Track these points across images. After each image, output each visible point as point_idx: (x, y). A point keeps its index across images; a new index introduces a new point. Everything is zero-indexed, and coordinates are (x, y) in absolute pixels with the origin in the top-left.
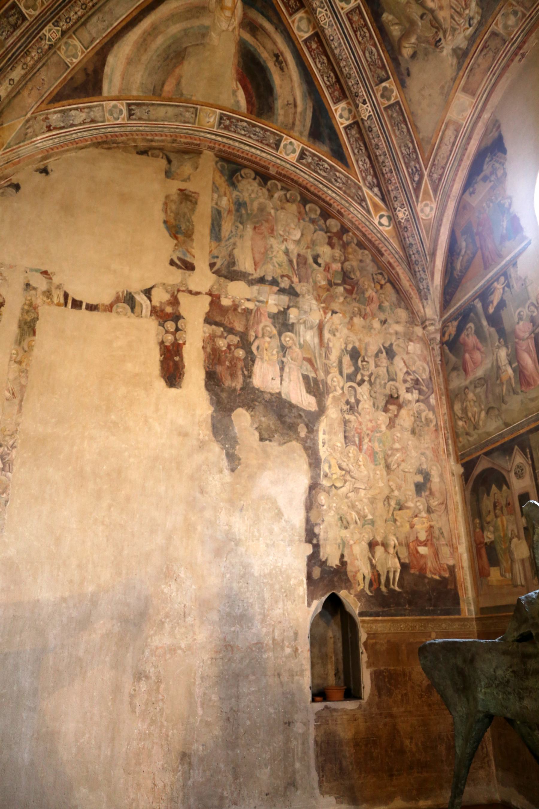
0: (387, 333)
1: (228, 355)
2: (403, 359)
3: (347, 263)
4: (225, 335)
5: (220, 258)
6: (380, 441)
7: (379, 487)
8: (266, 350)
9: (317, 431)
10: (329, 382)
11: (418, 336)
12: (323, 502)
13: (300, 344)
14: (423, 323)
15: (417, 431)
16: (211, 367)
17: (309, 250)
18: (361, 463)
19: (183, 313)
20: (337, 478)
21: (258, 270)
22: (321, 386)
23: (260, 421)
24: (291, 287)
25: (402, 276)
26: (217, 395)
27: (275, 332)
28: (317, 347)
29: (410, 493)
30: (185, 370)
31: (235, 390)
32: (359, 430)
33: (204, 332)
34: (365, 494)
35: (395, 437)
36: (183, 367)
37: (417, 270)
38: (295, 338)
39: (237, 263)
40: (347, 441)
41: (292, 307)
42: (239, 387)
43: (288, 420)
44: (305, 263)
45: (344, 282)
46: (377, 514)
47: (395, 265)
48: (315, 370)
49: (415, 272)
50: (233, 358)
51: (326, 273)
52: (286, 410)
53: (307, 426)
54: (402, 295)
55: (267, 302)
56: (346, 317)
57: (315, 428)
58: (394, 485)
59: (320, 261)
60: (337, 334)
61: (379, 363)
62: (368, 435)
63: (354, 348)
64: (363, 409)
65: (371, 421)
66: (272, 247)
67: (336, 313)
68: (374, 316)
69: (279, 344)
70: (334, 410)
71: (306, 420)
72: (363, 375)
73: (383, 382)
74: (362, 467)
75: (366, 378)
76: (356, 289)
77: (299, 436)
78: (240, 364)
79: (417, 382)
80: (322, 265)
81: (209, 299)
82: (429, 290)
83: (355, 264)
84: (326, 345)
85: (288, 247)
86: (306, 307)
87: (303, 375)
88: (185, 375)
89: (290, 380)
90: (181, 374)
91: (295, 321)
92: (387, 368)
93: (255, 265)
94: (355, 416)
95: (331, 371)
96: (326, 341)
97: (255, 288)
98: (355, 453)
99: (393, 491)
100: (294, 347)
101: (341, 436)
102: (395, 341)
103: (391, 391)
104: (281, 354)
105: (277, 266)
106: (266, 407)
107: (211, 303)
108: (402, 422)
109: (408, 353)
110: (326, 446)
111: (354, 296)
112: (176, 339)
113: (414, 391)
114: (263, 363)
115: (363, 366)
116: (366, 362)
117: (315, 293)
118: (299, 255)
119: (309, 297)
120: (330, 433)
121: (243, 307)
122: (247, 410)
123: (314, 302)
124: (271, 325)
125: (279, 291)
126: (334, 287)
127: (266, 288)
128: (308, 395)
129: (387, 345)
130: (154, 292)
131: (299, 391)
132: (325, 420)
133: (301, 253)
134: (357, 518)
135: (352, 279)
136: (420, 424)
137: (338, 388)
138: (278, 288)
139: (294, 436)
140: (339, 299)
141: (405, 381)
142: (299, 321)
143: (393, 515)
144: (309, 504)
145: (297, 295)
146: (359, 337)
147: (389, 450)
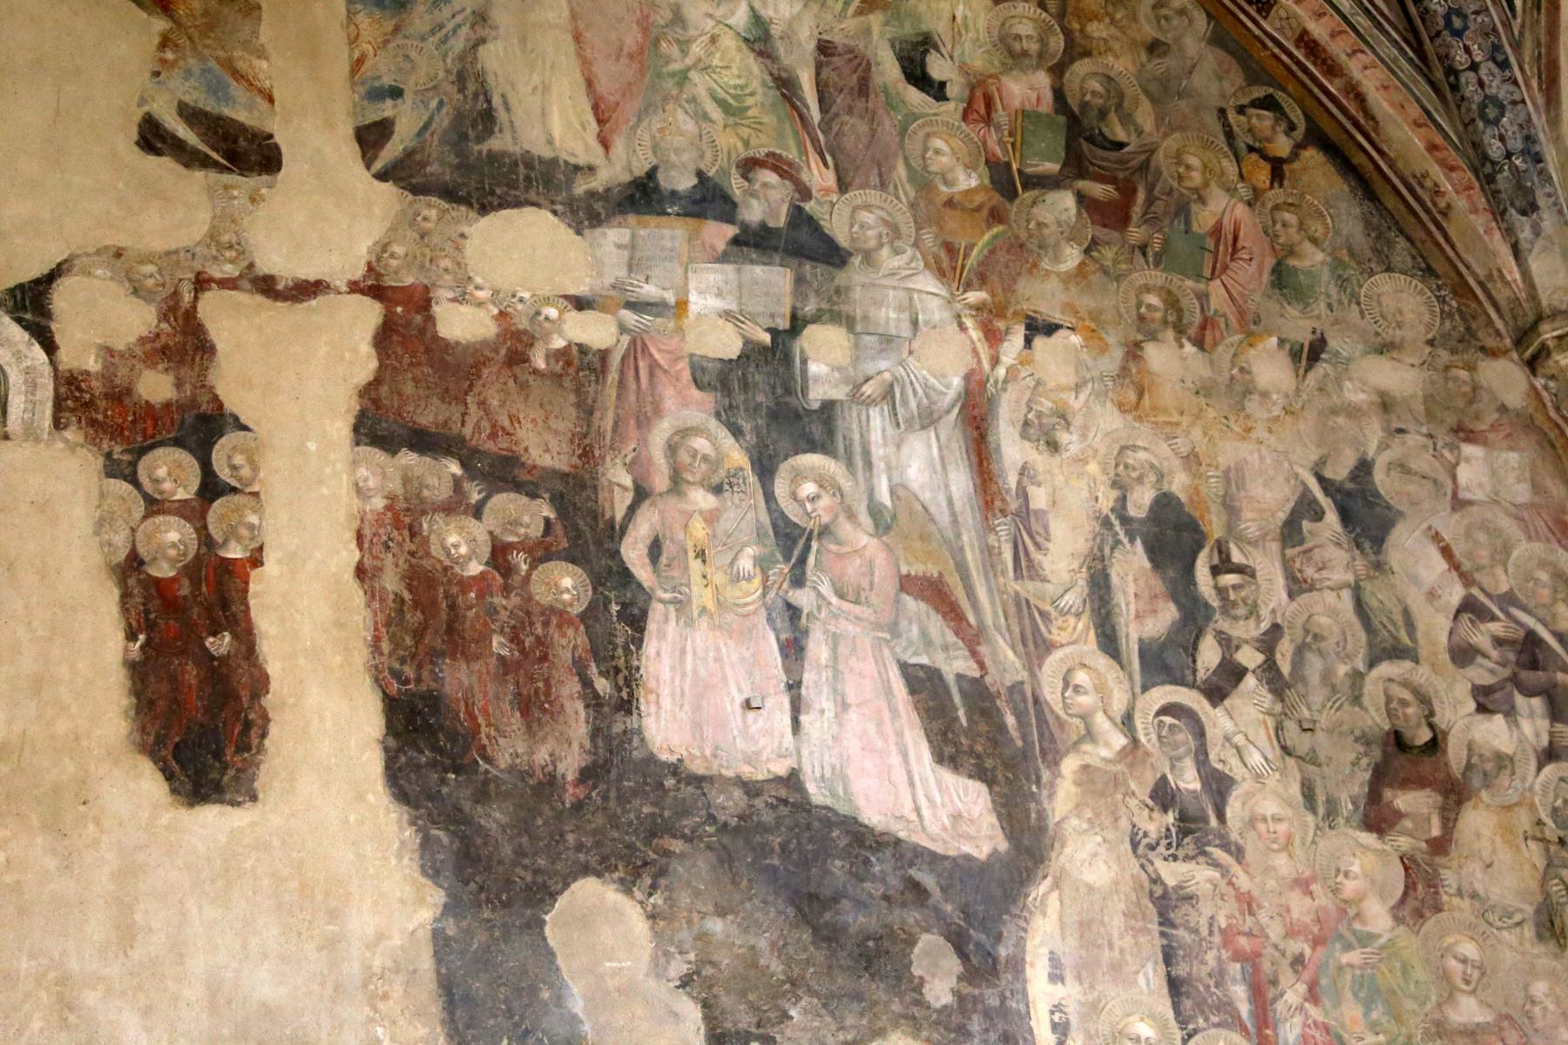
0: (1335, 411)
1: (498, 600)
2: (1436, 537)
3: (1080, 68)
4: (475, 497)
5: (409, 96)
6: (1369, 992)
8: (701, 555)
9: (1017, 965)
10: (1051, 692)
11: (1503, 408)
13: (875, 511)
14: (1523, 336)
16: (409, 671)
17: (875, 20)
19: (234, 400)
21: (619, 146)
22: (1010, 720)
23: (703, 937)
24: (799, 218)
25: (1380, 102)
26: (454, 818)
27: (737, 456)
28: (970, 519)
30: (268, 701)
31: (551, 782)
32: (1243, 941)
33: (360, 491)
35: (1453, 964)
36: (261, 683)
37: (1460, 58)
38: (846, 484)
39: (501, 115)
40: (1187, 1004)
41: (816, 319)
42: (570, 765)
43: (855, 920)
44: (863, 88)
45: (1076, 166)
47: (1338, 49)
48: (973, 639)
49: (1451, 71)
50: (527, 613)
51: (974, 131)
52: (837, 866)
53: (959, 942)
54: (1390, 202)
55: (682, 305)
56: (1104, 349)
57: (1003, 952)
59: (938, 68)
60: (1063, 437)
61: (1310, 572)
62: (1298, 961)
63: (1165, 502)
64: (1252, 822)
65: (1303, 885)
66: (678, 18)
67: (1050, 329)
68: (1251, 326)
69: (765, 518)
70: (1093, 842)
71: (949, 908)
72: (1225, 641)
73: (1342, 670)
75: (1249, 657)
76: (1141, 195)
77: (920, 1003)
78: (569, 643)
79: (1529, 651)
80: (951, 91)
81: (370, 314)
82: (1538, 159)
83: (1122, 65)
84: (1013, 505)
85: (767, 13)
86: (890, 316)
87: (905, 668)
88: (274, 730)
89: (844, 706)
90: (248, 725)
91: (839, 393)
92: (1357, 590)
93: (600, 121)
94: (1215, 864)
95: (1057, 636)
96: (1012, 481)
97: (613, 236)
100: (845, 528)
101: (1150, 979)
102: (1384, 446)
103: (1390, 714)
104: (782, 568)
105: (716, 113)
106: (726, 859)
107: (384, 338)
108: (1477, 878)
109: (1458, 504)
111: (1136, 233)
112: (206, 540)
113: (1520, 700)
114: (690, 623)
115: (1221, 591)
116: (1240, 570)
117: (928, 237)
118: (825, 49)
119: (897, 262)
120: (1086, 971)
121: (558, 343)
122: (627, 887)
123: (928, 283)
124: (713, 423)
125: (736, 241)
126: (1027, 196)
127: (668, 233)
128: (948, 777)
129: (1340, 471)
130: (62, 298)
131: (896, 760)
132: (1053, 901)
133: (838, 39)
135: (1120, 145)
137: (1101, 722)
138: (731, 231)
139: (896, 1007)
140: (1057, 259)
141: (1463, 655)
142: (857, 387)
145: (833, 255)
146: (1182, 445)
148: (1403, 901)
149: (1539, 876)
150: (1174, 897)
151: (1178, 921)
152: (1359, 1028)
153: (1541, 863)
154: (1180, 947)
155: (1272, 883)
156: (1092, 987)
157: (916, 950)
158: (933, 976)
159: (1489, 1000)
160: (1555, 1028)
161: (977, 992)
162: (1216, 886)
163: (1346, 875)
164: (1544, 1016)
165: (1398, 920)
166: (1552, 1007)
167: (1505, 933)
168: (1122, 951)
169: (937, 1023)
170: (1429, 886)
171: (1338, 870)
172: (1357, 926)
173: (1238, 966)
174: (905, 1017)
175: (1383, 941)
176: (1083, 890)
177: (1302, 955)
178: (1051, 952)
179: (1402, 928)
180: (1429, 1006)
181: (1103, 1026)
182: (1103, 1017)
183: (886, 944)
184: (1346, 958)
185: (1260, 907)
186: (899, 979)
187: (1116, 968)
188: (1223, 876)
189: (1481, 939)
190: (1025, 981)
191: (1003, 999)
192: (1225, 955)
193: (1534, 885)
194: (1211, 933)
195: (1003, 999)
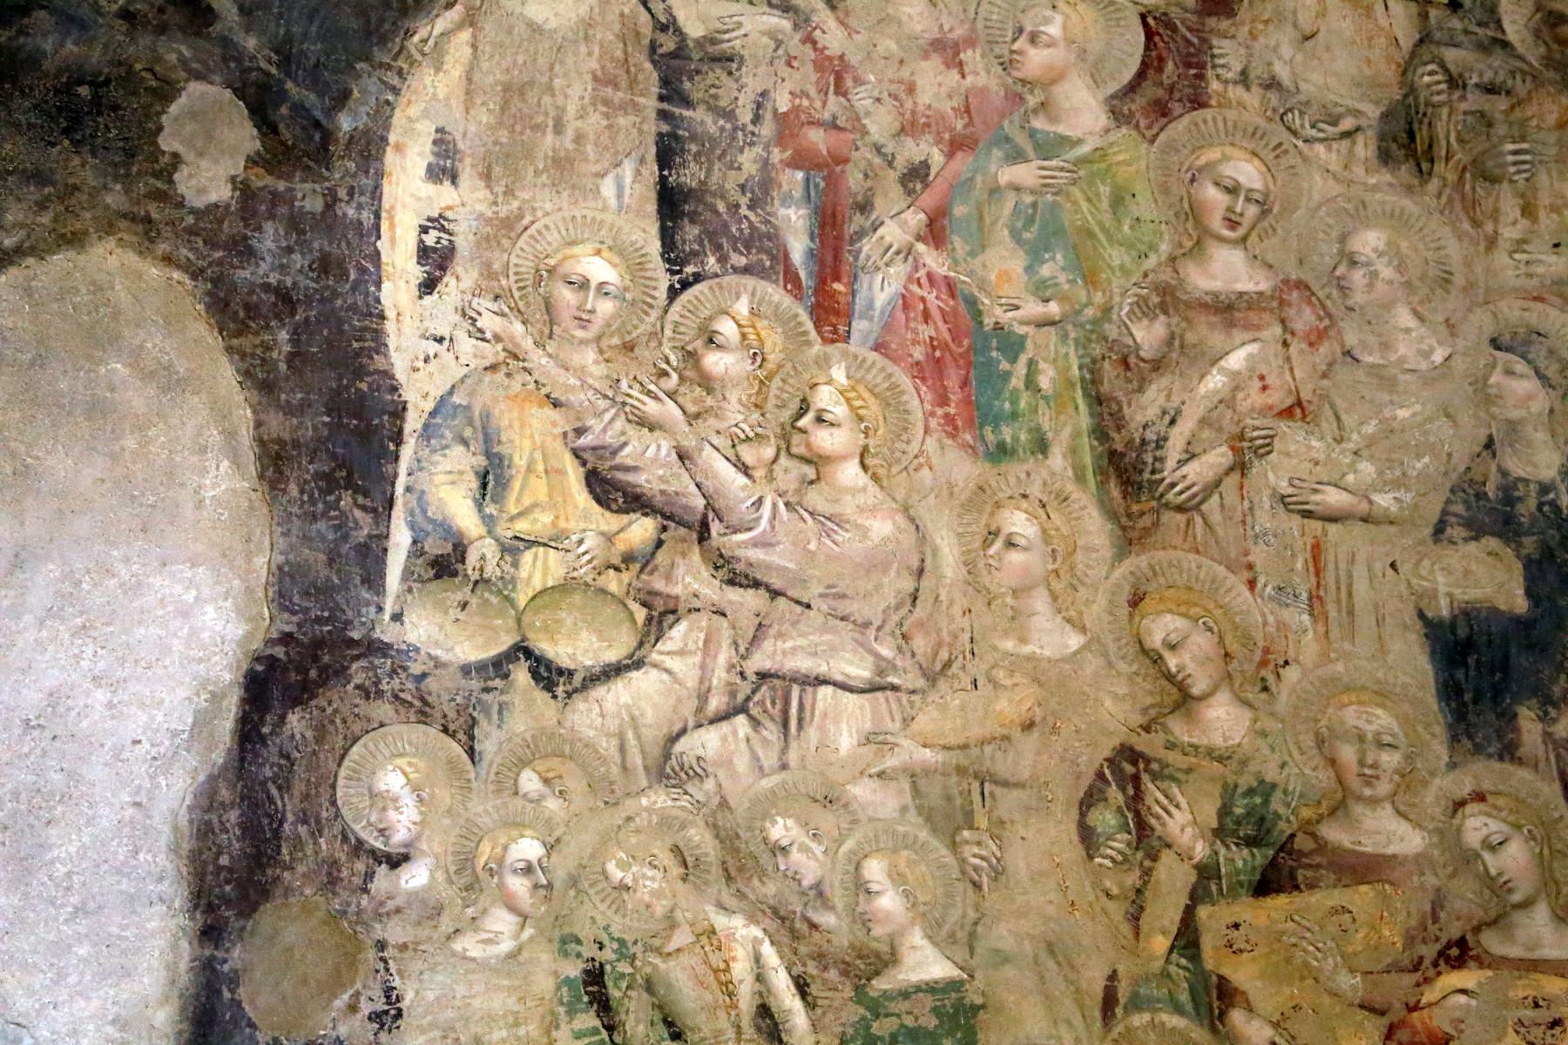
7: (1035, 670)
12: (403, 822)
15: (1445, 128)
18: (826, 440)
20: (566, 587)
29: (1382, 720)
34: (874, 739)
35: (1212, 195)
40: (690, 232)
46: (1002, 936)
57: (345, 123)
58: (1201, 642)
62: (916, 175)
71: (251, 43)
74: (850, 473)
98: (774, 342)
99: (1183, 700)
108: (1284, 60)
110: (453, 288)
134: (781, 982)
136: (1491, 68)
139: (115, 198)
143: (1187, 939)
144: (232, 844)
147: (1143, 309)
148: (1133, 87)
149: (1401, 56)
150: (696, 56)
151: (696, 96)
152: (1017, 287)
153: (1407, 35)
154: (693, 138)
155: (888, 45)
156: (509, 192)
157: (174, 109)
158: (201, 154)
159: (1270, 258)
160: (1388, 306)
161: (281, 186)
162: (779, 44)
163: (1034, 39)
164: (1370, 286)
165: (1118, 115)
166: (1386, 272)
167: (1320, 148)
168: (579, 138)
169: (192, 232)
170: (1189, 65)
171: (1021, 31)
172: (1039, 123)
173: (800, 175)
174: (132, 218)
175: (1085, 149)
176: (520, 29)
177: (925, 165)
178: (439, 130)
179: (1124, 130)
180: (1152, 261)
181: (521, 258)
182: (521, 243)
183: (115, 93)
184: (1007, 175)
185: (858, 82)
186: (130, 154)
187: (562, 165)
188: (796, 26)
189: (1272, 157)
190: (380, 174)
191: (331, 201)
192: (777, 155)
193: (1389, 73)
194: (757, 119)
195: (330, 205)
